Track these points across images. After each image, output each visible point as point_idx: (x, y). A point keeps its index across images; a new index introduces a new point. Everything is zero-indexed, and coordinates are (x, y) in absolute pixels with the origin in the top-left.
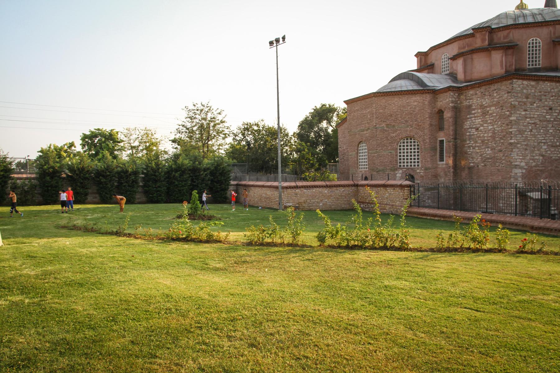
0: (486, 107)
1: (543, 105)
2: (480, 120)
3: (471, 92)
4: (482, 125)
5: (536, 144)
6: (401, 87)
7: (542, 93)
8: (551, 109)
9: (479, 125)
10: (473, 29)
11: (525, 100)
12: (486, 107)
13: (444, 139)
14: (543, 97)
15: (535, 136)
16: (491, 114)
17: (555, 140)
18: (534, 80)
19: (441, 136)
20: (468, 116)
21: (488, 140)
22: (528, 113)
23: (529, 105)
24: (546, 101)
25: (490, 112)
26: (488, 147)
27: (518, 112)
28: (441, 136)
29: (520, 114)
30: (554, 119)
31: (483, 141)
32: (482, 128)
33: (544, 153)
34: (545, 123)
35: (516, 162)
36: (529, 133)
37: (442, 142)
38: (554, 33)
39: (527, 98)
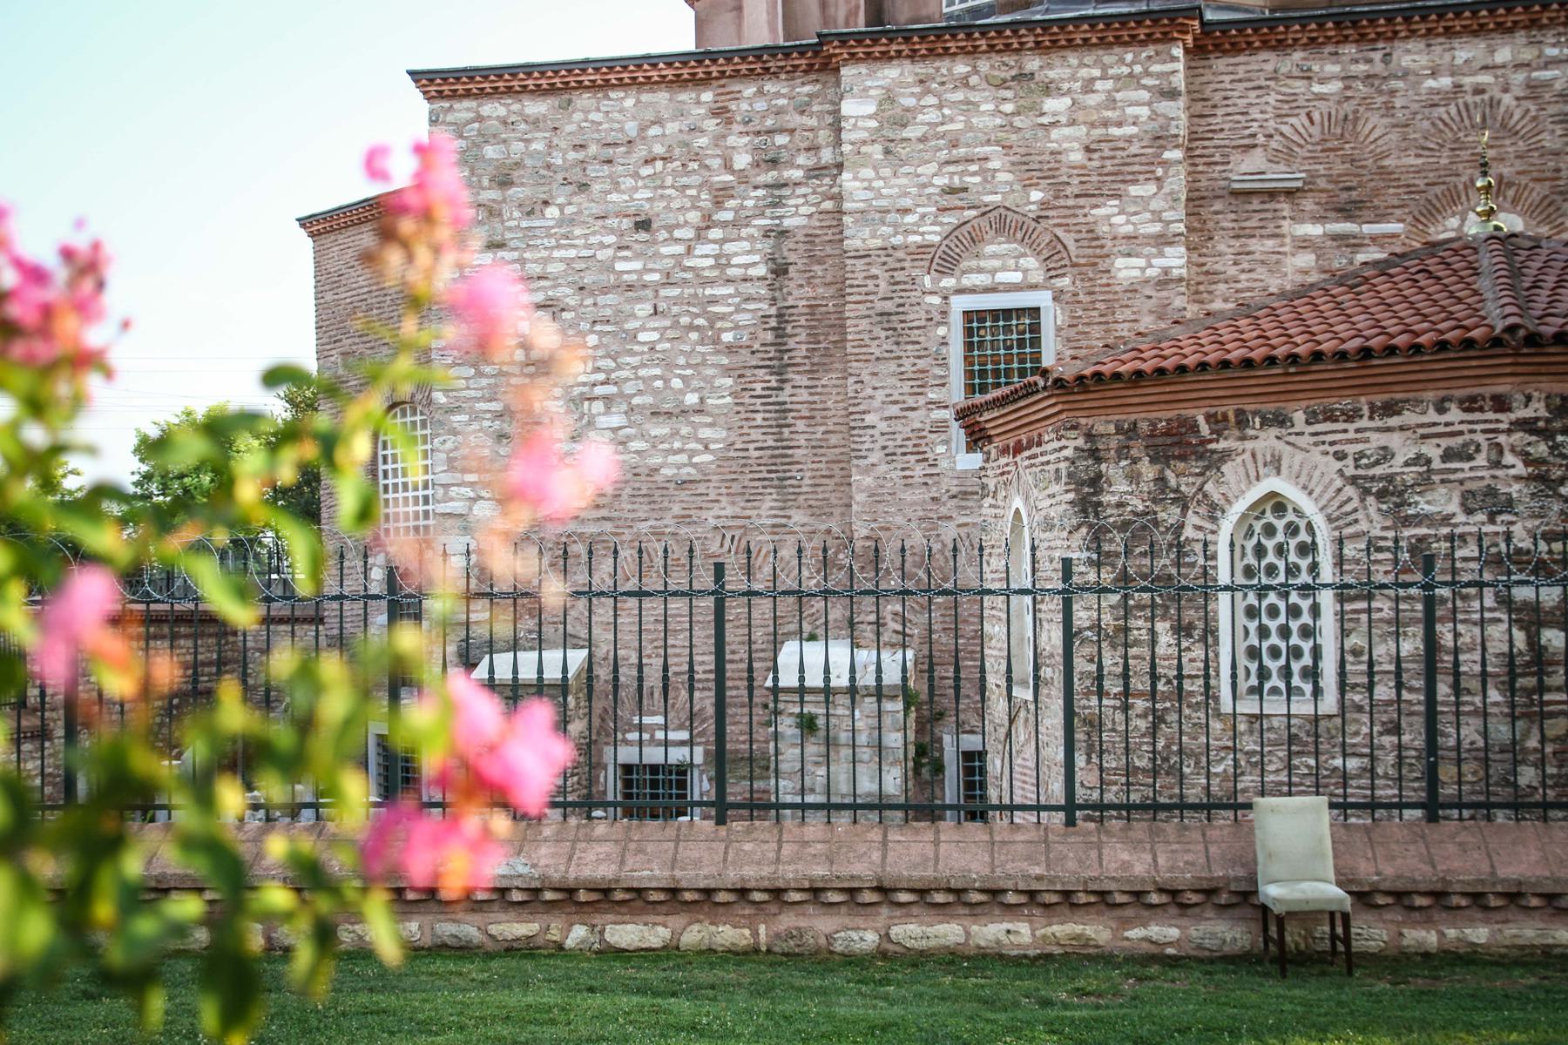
1: (596, 209)
7: (593, 149)
8: (644, 225)
11: (493, 194)
14: (593, 170)
17: (677, 383)
18: (539, 91)
23: (513, 217)
34: (611, 298)
35: (447, 499)
39: (505, 183)
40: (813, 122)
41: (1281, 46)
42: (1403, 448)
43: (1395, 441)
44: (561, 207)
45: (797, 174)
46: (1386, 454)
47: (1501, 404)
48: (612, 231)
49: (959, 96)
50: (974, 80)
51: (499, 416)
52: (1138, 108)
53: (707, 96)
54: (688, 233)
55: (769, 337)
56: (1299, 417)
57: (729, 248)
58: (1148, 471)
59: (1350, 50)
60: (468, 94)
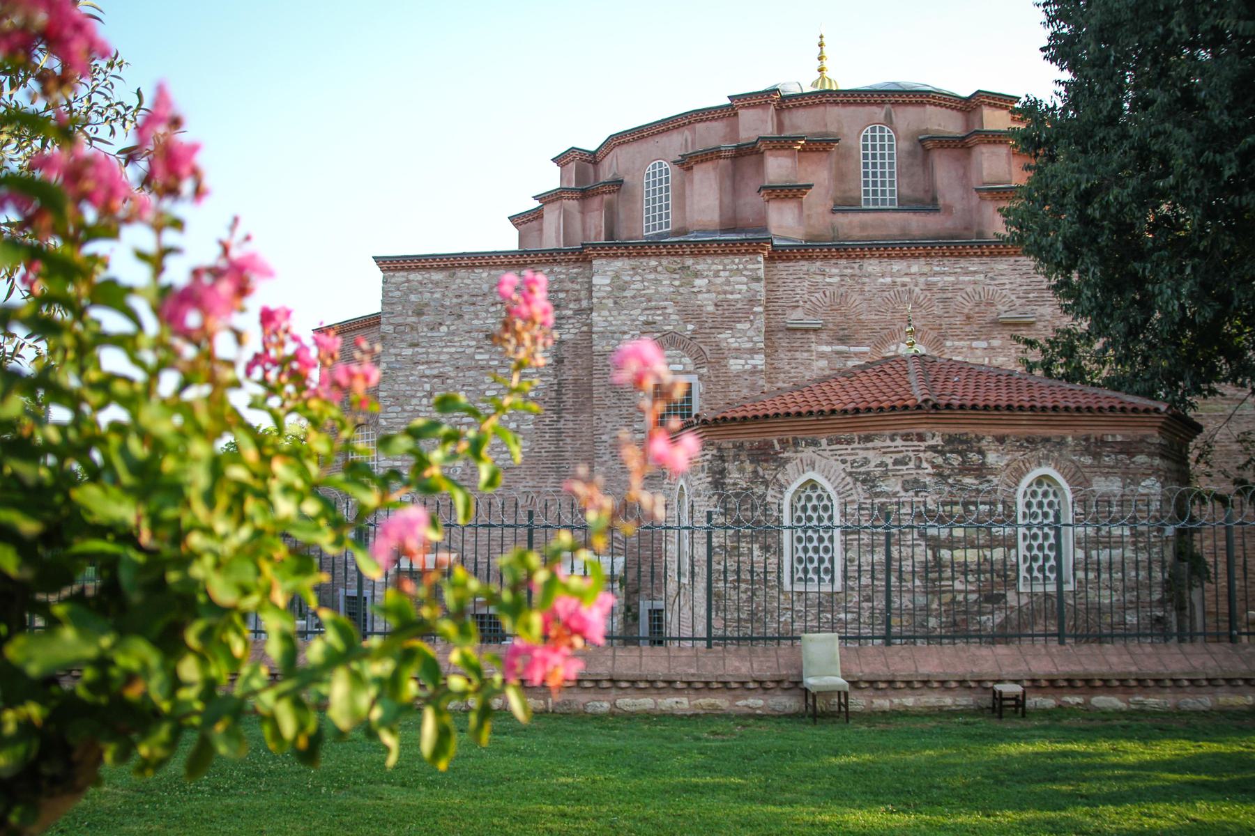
1: (466, 328)
7: (466, 298)
11: (414, 319)
14: (465, 308)
18: (439, 268)
22: (420, 350)
27: (392, 351)
29: (396, 355)
34: (472, 373)
36: (425, 401)
38: (693, 143)
39: (420, 313)
40: (578, 287)
41: (810, 258)
42: (874, 458)
43: (870, 455)
44: (448, 326)
45: (570, 313)
46: (866, 461)
47: (921, 438)
48: (474, 339)
49: (652, 276)
50: (659, 269)
52: (741, 287)
55: (553, 394)
56: (824, 442)
58: (749, 467)
59: (843, 262)
60: (403, 269)
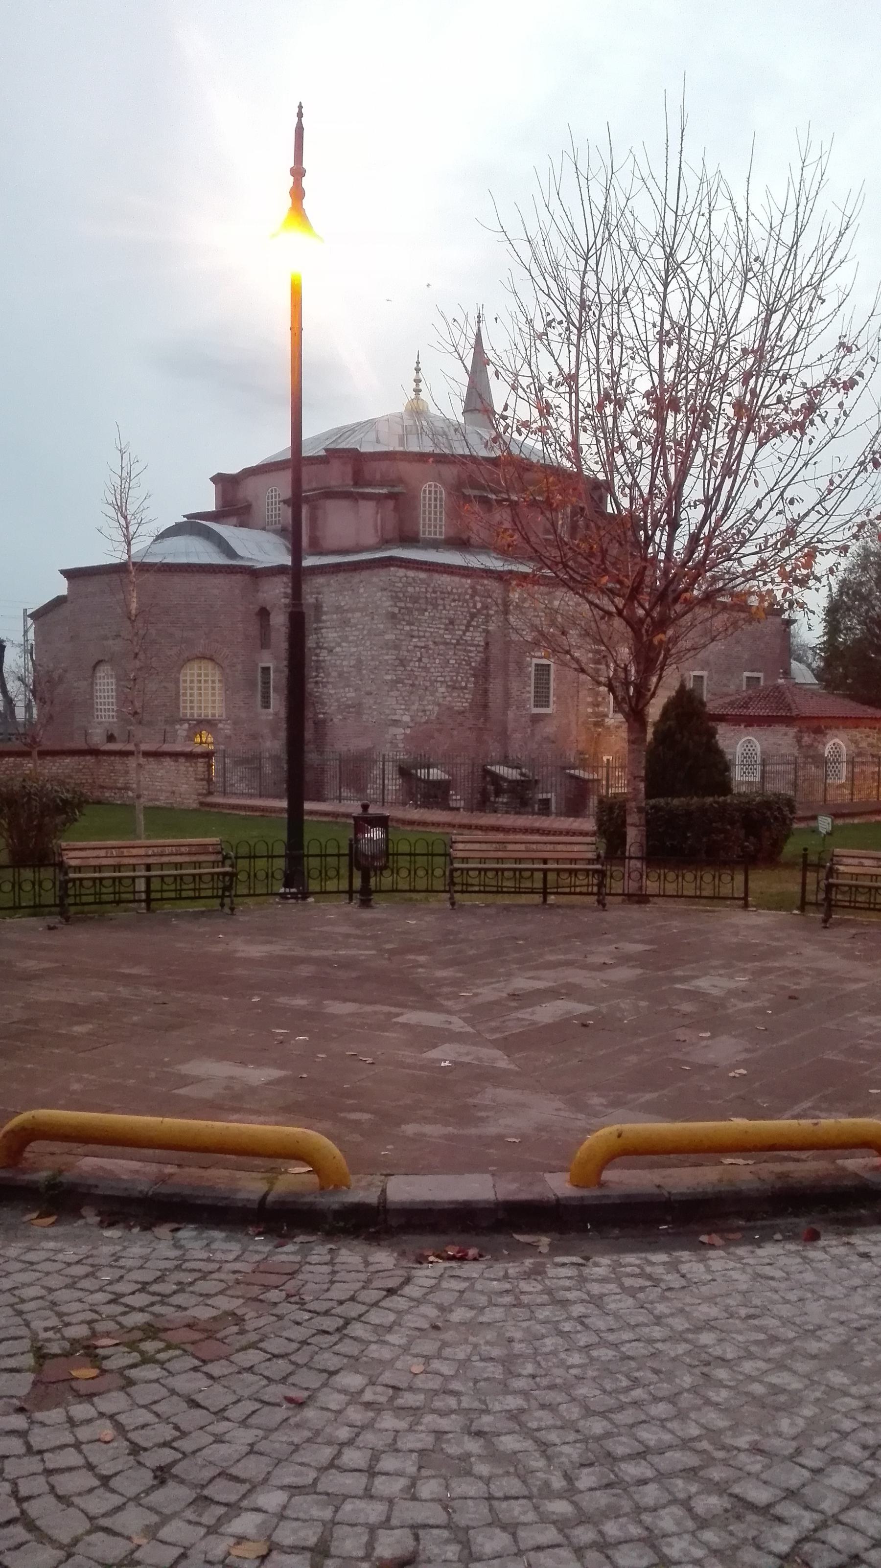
0: (347, 611)
1: (438, 615)
2: (335, 635)
3: (321, 580)
4: (339, 645)
5: (428, 684)
6: (187, 554)
9: (333, 644)
10: (326, 450)
12: (347, 611)
13: (271, 665)
14: (440, 602)
15: (425, 669)
16: (355, 625)
18: (426, 570)
19: (267, 660)
20: (315, 625)
21: (349, 673)
24: (445, 609)
25: (352, 621)
26: (349, 686)
28: (267, 660)
30: (458, 640)
31: (340, 675)
32: (338, 649)
33: (441, 700)
34: (442, 647)
37: (266, 670)
42: (858, 736)
51: (413, 685)
53: (469, 581)
54: (463, 628)
57: (476, 634)
